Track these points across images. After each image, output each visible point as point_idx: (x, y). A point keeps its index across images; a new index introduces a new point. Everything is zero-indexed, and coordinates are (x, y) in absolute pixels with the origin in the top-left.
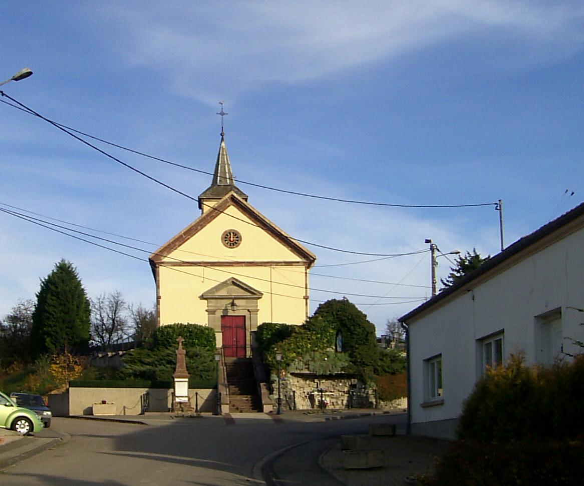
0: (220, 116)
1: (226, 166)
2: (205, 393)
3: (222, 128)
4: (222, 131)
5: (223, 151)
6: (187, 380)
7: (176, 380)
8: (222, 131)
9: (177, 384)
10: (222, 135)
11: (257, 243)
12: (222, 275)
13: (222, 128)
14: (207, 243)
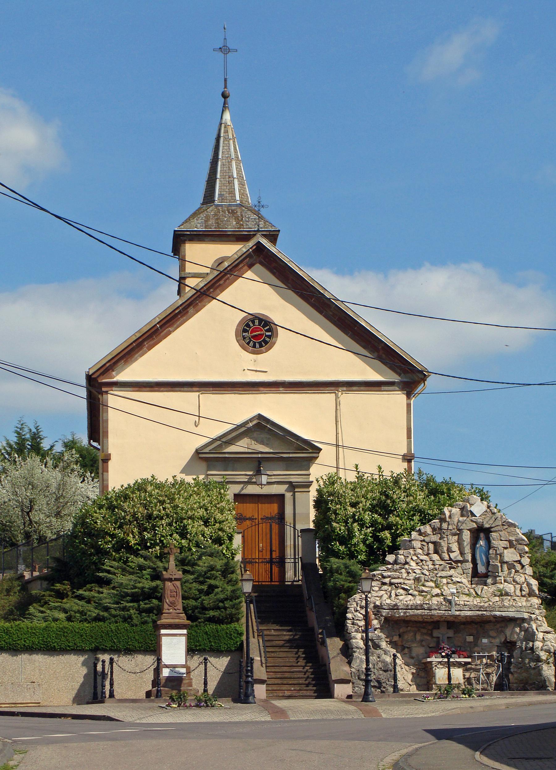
0: (221, 55)
1: (236, 182)
2: (219, 664)
3: (225, 80)
4: (226, 87)
5: (226, 132)
6: (185, 631)
7: (163, 631)
8: (226, 87)
9: (165, 641)
10: (225, 96)
11: (306, 347)
12: (241, 409)
13: (225, 80)
14: (205, 344)
